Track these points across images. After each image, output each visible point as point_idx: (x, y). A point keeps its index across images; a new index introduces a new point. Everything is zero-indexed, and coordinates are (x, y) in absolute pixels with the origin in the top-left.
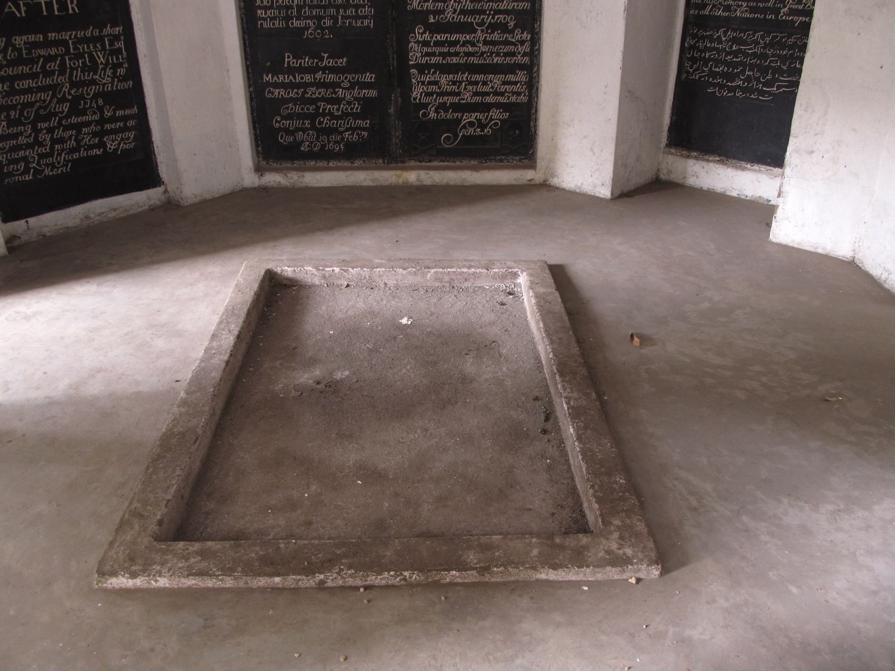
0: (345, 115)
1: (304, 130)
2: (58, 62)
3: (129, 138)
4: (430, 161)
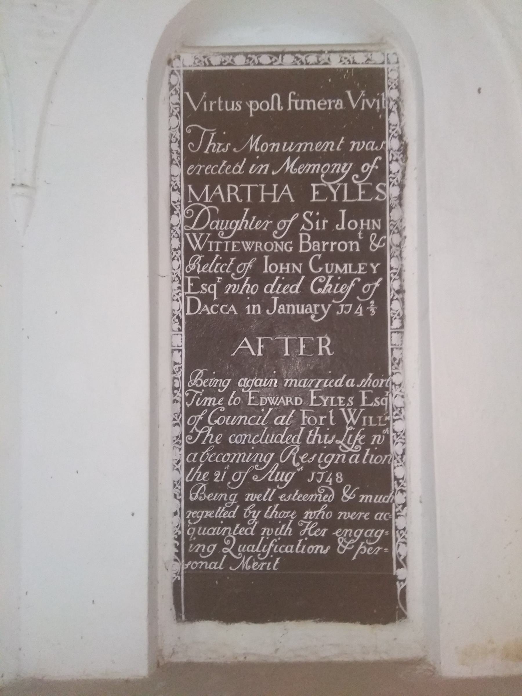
3: (373, 539)
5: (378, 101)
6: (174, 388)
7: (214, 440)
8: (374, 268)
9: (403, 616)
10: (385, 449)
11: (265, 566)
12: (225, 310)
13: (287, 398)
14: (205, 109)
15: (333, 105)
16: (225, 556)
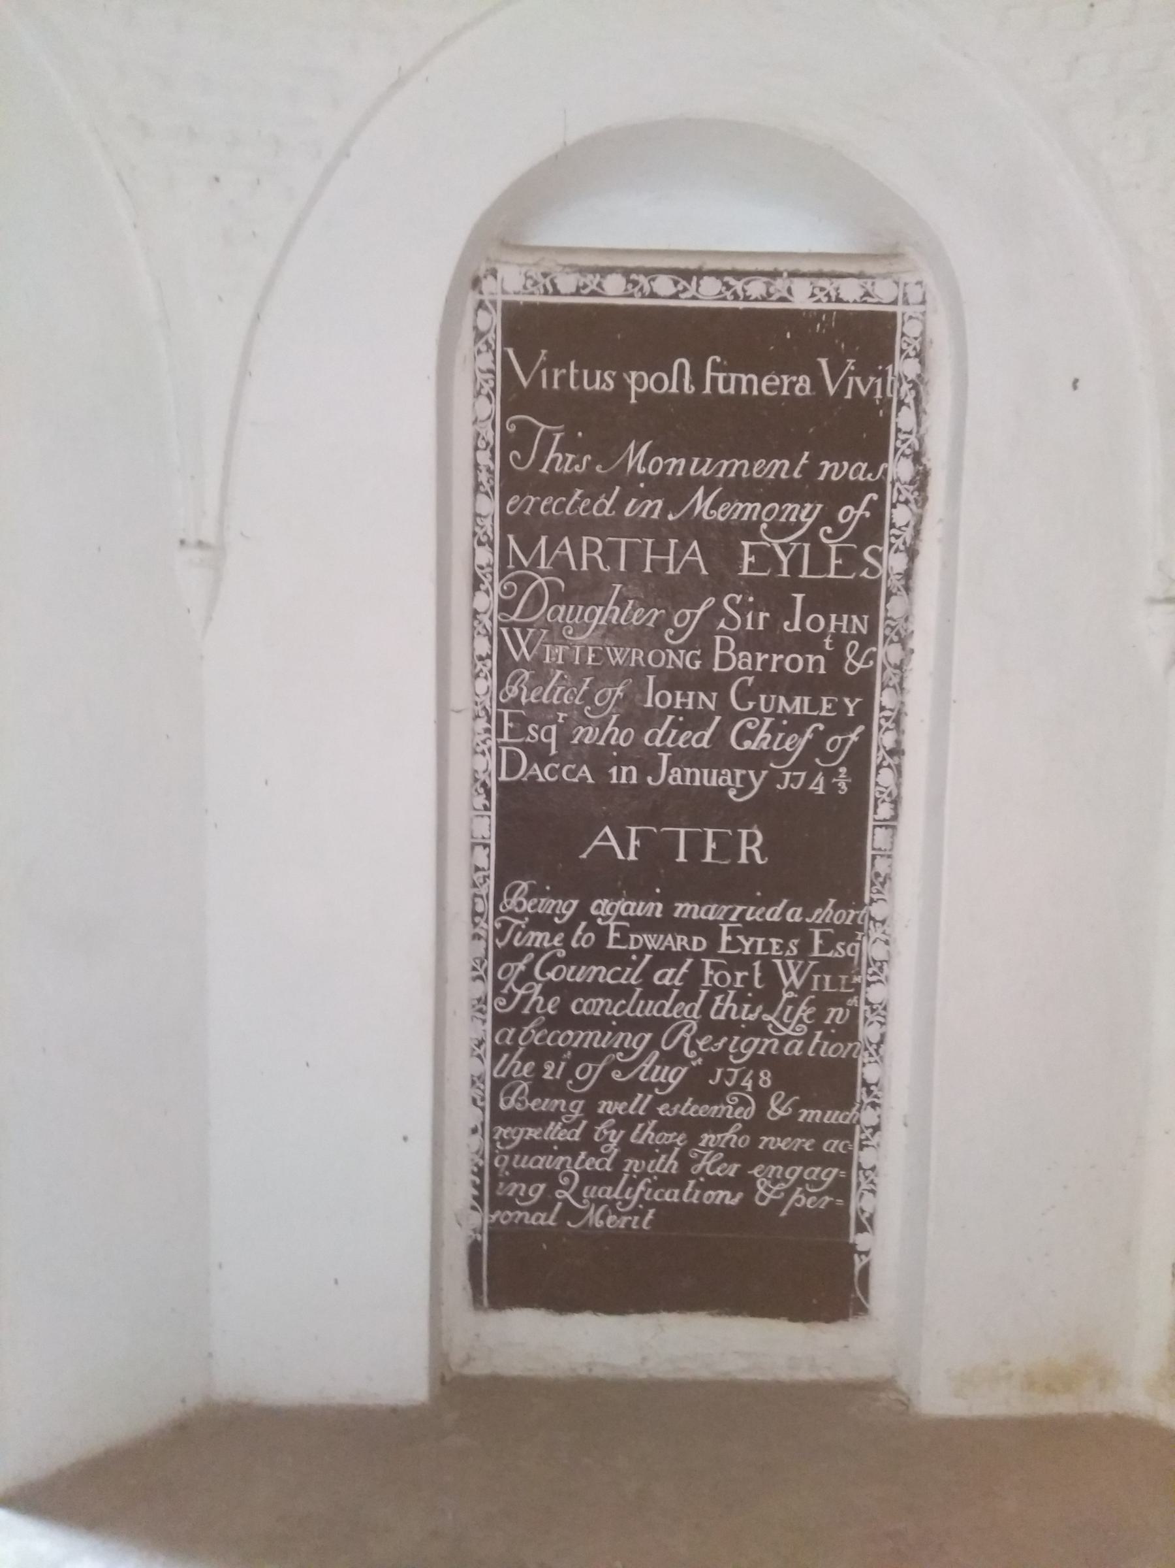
2: (684, 970)
3: (819, 1183)
5: (879, 381)
6: (475, 914)
7: (545, 1006)
8: (851, 707)
9: (861, 1309)
10: (848, 1032)
11: (629, 1222)
13: (679, 937)
14: (544, 385)
15: (792, 385)
16: (559, 1204)
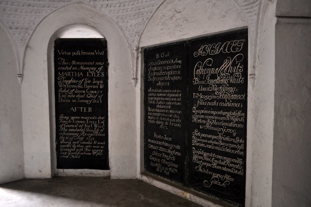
0: (170, 161)
1: (158, 163)
3: (100, 152)
4: (199, 191)
12: (67, 101)
15: (92, 53)
